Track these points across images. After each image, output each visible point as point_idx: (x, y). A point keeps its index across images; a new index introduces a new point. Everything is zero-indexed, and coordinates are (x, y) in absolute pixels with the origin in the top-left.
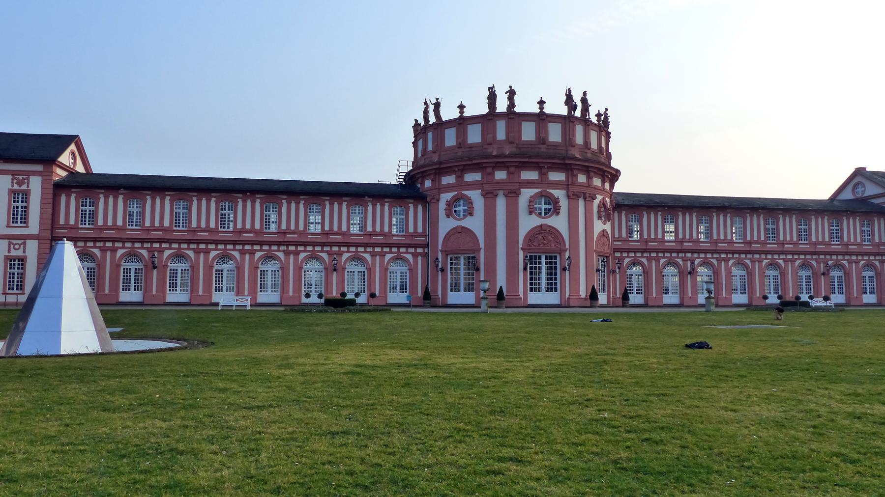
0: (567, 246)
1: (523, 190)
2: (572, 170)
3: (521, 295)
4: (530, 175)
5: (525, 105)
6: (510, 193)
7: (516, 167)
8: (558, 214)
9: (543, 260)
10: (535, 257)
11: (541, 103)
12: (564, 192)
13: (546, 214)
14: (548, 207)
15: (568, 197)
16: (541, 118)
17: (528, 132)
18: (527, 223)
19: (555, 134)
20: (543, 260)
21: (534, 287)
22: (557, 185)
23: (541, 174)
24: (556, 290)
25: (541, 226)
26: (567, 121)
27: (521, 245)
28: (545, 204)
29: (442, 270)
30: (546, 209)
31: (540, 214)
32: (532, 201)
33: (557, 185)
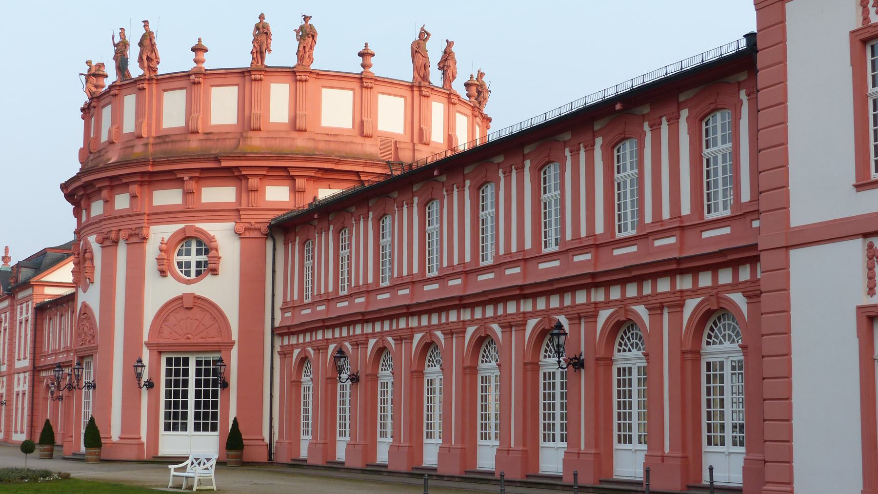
0: (235, 337)
1: (154, 229)
2: (293, 178)
3: (144, 439)
4: (167, 197)
5: (173, 59)
6: (130, 235)
7: (141, 184)
8: (214, 272)
9: (192, 368)
10: (177, 361)
11: (198, 49)
12: (230, 225)
13: (198, 273)
14: (203, 258)
15: (239, 235)
16: (195, 80)
17: (173, 110)
18: (159, 292)
19: (223, 107)
20: (192, 368)
21: (175, 422)
22: (216, 213)
23: (187, 193)
24: (214, 428)
25: (180, 298)
26: (251, 77)
27: (145, 339)
28: (199, 252)
29: (150, 385)
30: (199, 264)
31: (188, 273)
32: (166, 249)
33: (216, 213)
